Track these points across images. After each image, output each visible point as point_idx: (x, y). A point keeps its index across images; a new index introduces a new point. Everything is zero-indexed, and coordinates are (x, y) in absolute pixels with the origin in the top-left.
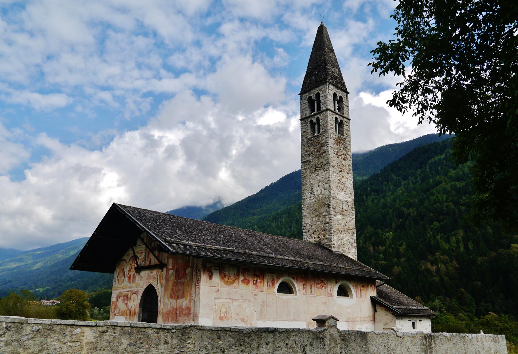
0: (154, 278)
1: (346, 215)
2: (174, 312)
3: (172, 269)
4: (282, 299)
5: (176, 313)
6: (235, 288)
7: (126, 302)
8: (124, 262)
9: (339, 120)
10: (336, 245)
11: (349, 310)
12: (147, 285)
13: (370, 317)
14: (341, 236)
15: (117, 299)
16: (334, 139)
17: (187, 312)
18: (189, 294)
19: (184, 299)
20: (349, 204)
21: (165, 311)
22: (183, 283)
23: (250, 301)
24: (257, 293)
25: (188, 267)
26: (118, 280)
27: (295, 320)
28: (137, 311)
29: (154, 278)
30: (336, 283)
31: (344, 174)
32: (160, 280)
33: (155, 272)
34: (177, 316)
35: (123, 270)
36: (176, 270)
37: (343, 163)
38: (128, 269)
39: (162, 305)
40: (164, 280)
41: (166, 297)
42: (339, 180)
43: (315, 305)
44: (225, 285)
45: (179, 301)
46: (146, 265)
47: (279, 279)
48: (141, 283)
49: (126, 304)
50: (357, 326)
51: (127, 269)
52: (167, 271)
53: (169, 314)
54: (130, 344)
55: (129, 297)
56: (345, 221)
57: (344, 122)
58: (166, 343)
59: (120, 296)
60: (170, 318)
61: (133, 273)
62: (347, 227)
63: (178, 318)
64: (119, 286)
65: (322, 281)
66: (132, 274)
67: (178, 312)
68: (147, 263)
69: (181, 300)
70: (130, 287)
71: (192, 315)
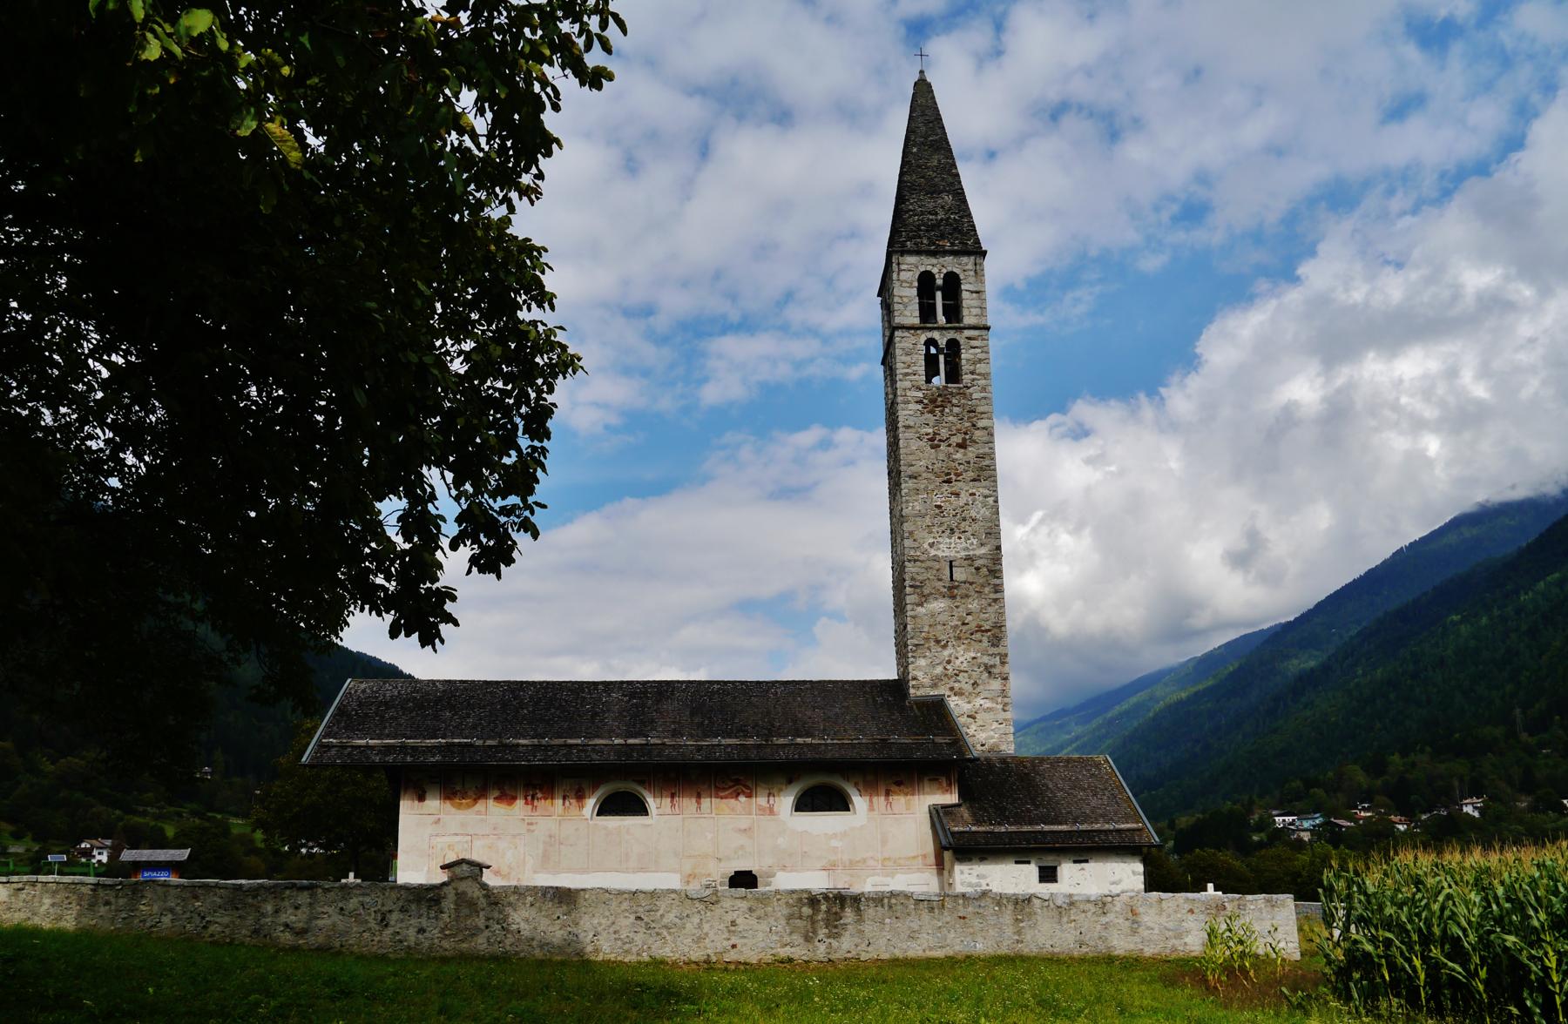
1: (967, 596)
4: (605, 828)
6: (478, 813)
9: (942, 342)
10: (927, 681)
11: (834, 843)
13: (925, 856)
14: (946, 653)
16: (920, 402)
20: (978, 563)
23: (514, 836)
24: (534, 820)
27: (643, 869)
30: (790, 782)
31: (956, 486)
37: (958, 456)
42: (939, 507)
43: (709, 836)
44: (453, 810)
47: (595, 787)
50: (870, 881)
54: (53, 905)
56: (962, 612)
57: (962, 341)
58: (107, 903)
62: (973, 626)
65: (737, 782)
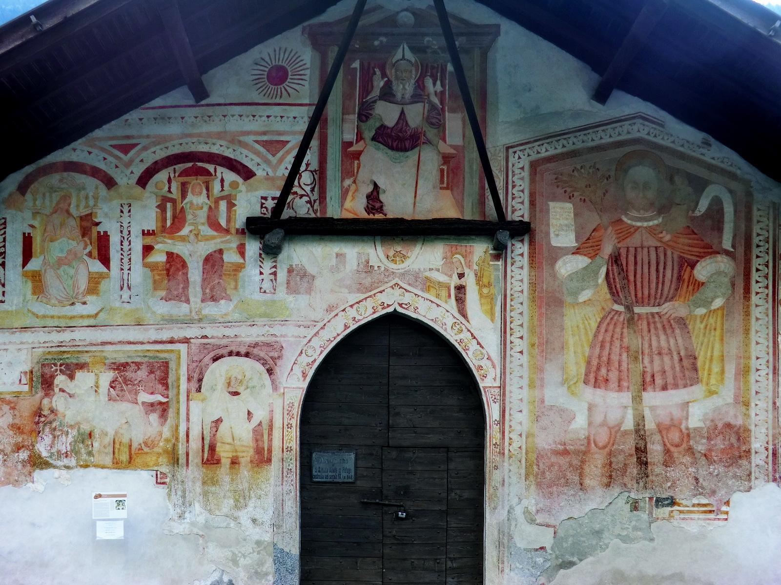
0: (428, 284)
2: (629, 445)
3: (577, 251)
5: (641, 452)
7: (144, 397)
8: (91, 182)
12: (367, 314)
15: (43, 380)
17: (719, 443)
18: (731, 370)
19: (697, 391)
21: (545, 441)
22: (682, 322)
25: (710, 251)
26: (36, 278)
28: (287, 438)
29: (428, 284)
32: (487, 299)
33: (428, 258)
34: (643, 463)
35: (87, 224)
36: (615, 259)
38: (146, 216)
39: (520, 420)
40: (525, 297)
41: (552, 374)
45: (660, 404)
46: (334, 211)
48: (298, 304)
49: (163, 409)
51: (130, 220)
52: (542, 258)
53: (583, 455)
55: (181, 372)
59: (71, 370)
60: (595, 469)
61: (205, 248)
63: (658, 469)
64: (40, 308)
66: (193, 250)
67: (655, 449)
68: (355, 207)
69: (676, 396)
70: (171, 320)
71: (758, 460)
